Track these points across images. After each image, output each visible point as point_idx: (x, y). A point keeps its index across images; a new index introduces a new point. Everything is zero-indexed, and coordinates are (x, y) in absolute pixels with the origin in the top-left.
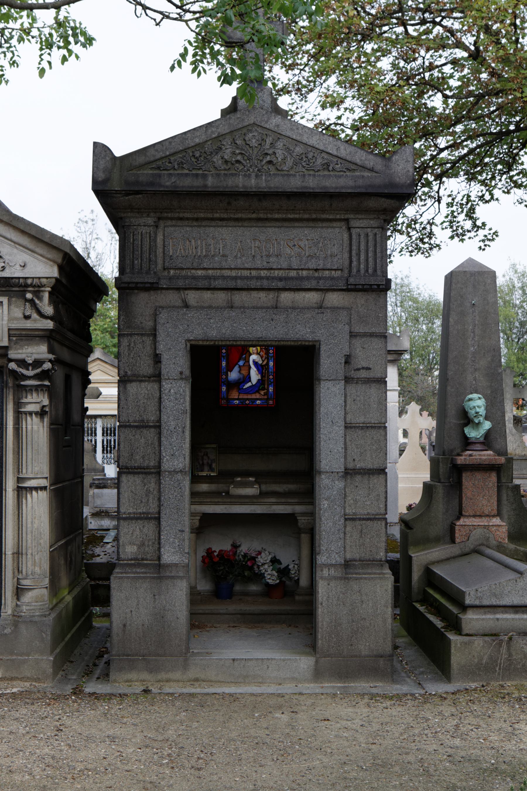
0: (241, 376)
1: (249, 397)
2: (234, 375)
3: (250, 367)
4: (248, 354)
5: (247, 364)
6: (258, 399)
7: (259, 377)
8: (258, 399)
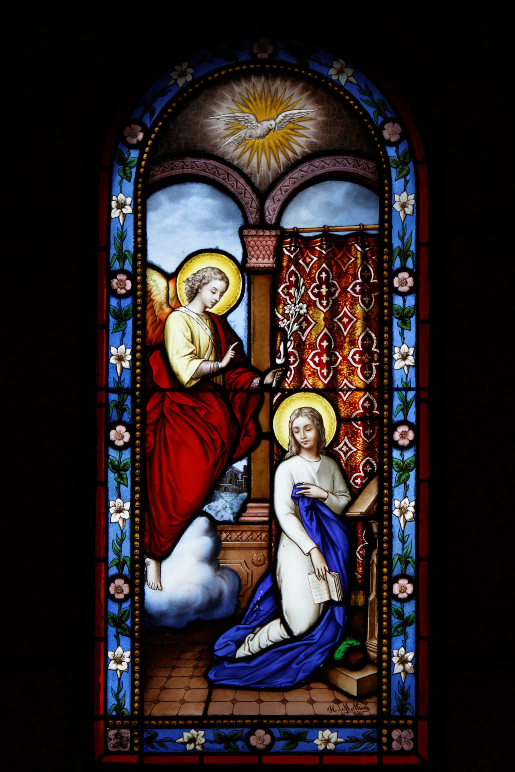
0: (225, 585)
1: (272, 706)
2: (182, 576)
3: (274, 532)
4: (262, 451)
5: (256, 513)
6: (322, 722)
7: (330, 589)
8: (322, 722)
